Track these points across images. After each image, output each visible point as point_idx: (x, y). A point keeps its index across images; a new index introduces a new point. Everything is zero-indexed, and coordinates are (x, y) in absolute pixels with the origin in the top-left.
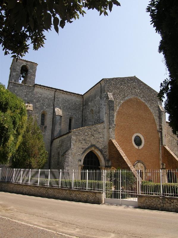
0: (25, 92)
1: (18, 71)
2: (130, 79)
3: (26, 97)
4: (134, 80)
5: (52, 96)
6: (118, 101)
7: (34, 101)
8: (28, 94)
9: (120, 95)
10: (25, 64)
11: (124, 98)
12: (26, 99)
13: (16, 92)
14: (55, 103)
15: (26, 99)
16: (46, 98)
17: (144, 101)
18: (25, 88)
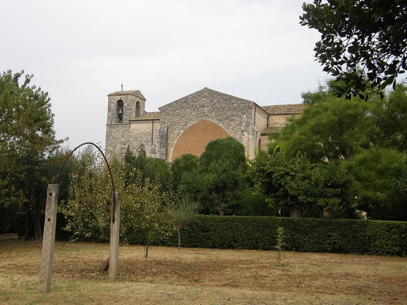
0: (121, 132)
1: (113, 110)
2: (197, 95)
3: (122, 138)
4: (207, 94)
5: (149, 130)
6: (176, 132)
7: (131, 140)
8: (125, 134)
9: (179, 123)
10: (119, 98)
11: (185, 125)
12: (123, 139)
13: (113, 134)
14: (153, 137)
15: (123, 139)
16: (144, 134)
17: (216, 122)
18: (121, 128)
